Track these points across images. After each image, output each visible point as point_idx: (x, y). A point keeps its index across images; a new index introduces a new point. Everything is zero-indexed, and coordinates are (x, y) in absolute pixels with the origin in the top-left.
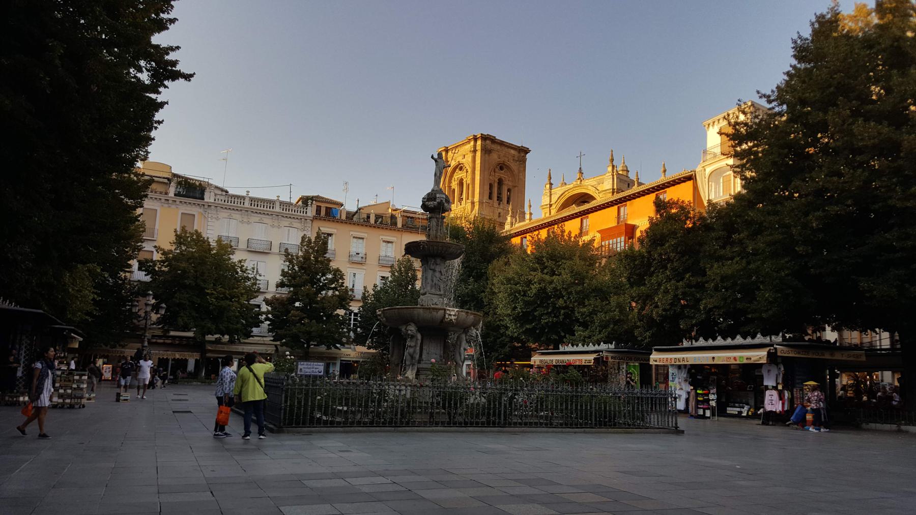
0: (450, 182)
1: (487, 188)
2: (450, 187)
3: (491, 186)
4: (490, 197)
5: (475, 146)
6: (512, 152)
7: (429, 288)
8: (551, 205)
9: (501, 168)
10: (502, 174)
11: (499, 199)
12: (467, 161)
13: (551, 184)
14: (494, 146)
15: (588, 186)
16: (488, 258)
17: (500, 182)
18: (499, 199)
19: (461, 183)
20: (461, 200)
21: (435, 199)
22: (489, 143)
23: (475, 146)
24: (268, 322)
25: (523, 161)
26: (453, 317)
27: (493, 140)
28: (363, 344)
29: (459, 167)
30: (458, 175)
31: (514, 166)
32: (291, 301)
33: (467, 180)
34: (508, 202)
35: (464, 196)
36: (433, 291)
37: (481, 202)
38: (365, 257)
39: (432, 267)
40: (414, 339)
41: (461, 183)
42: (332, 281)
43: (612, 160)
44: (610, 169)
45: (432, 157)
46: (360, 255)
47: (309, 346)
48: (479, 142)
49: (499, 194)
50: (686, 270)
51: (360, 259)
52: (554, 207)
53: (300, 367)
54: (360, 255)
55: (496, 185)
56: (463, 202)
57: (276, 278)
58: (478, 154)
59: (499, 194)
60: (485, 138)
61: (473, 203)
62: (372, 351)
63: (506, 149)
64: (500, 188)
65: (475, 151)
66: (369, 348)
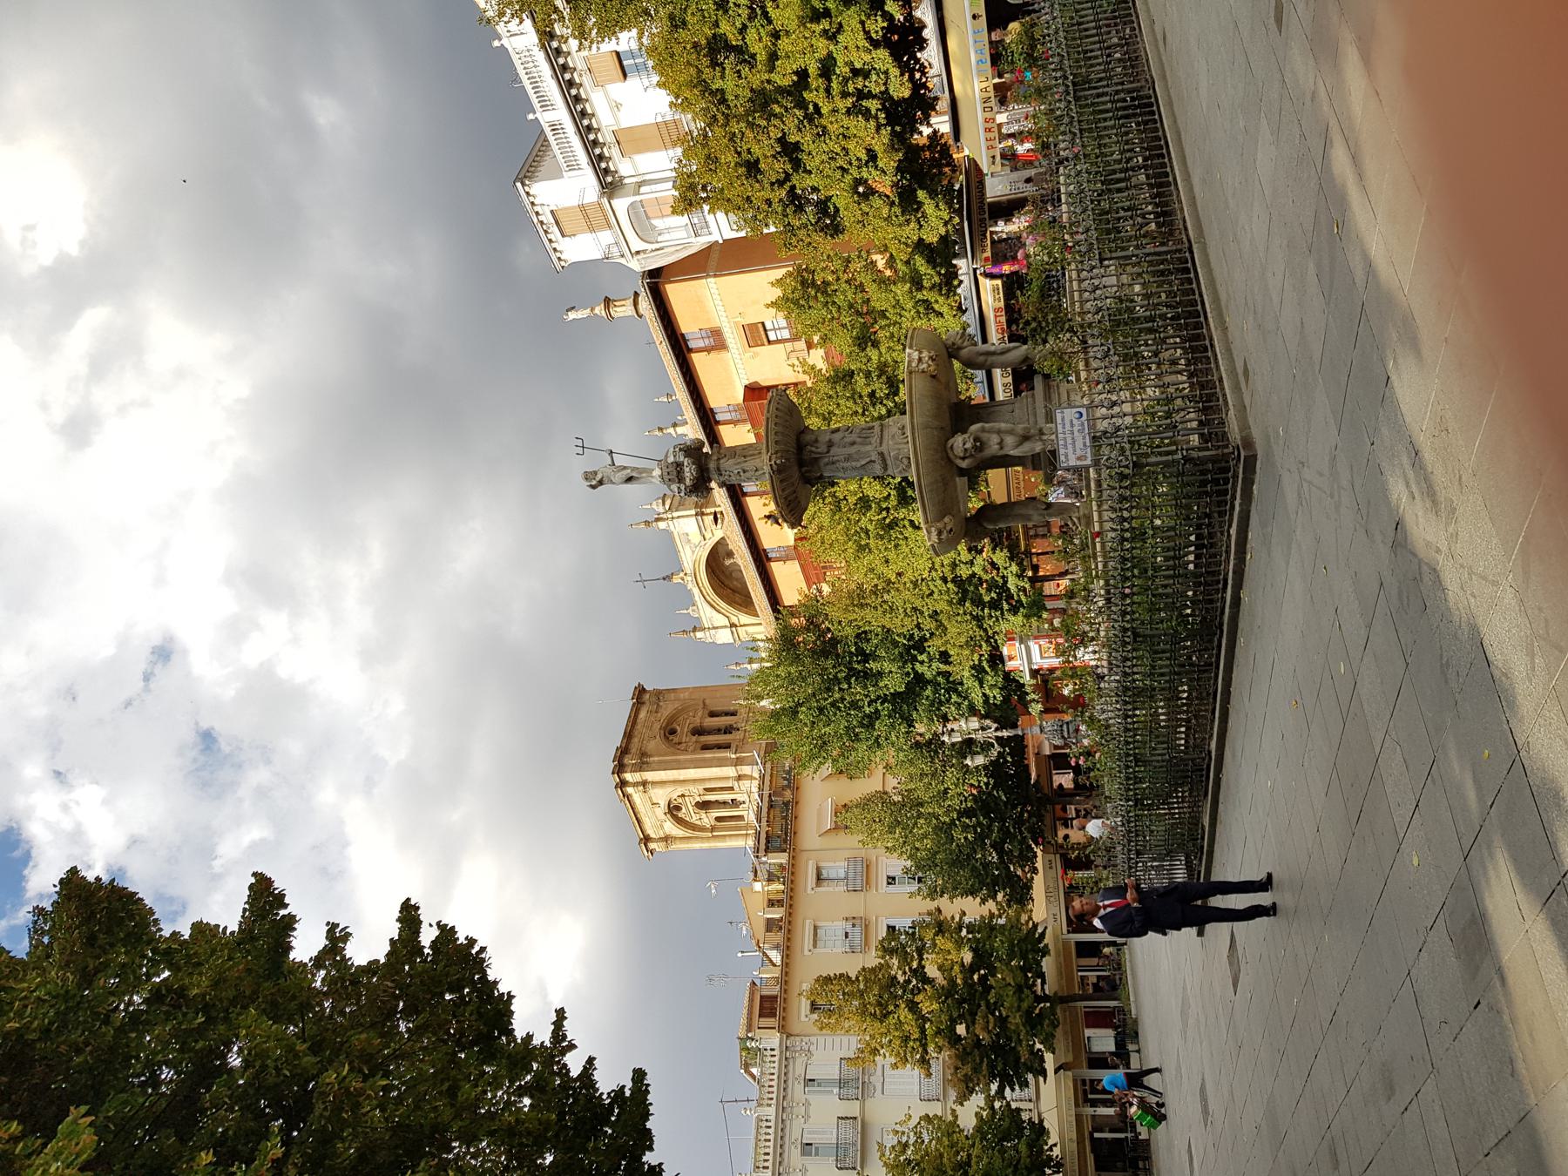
0: (702, 829)
1: (708, 755)
2: (713, 829)
3: (706, 748)
4: (727, 747)
5: (636, 785)
6: (642, 715)
7: (869, 448)
8: (733, 625)
9: (673, 732)
10: (683, 730)
11: (728, 730)
12: (662, 796)
13: (695, 630)
14: (634, 747)
15: (693, 556)
16: (828, 647)
17: (699, 732)
18: (728, 730)
19: (704, 806)
20: (735, 803)
21: (679, 465)
22: (628, 756)
23: (636, 785)
24: (1008, 1091)
25: (659, 694)
26: (925, 354)
27: (623, 751)
28: (1028, 887)
29: (673, 810)
30: (689, 812)
31: (667, 710)
32: (955, 1040)
33: (696, 793)
34: (733, 714)
35: (727, 797)
36: (875, 440)
37: (738, 762)
38: (853, 920)
39: (823, 448)
40: (985, 436)
41: (704, 806)
42: (905, 959)
43: (647, 523)
44: (662, 525)
45: (593, 487)
46: (849, 928)
47: (1045, 998)
48: (628, 776)
49: (718, 731)
50: (802, 104)
51: (857, 929)
52: (734, 620)
53: (1073, 462)
54: (849, 928)
55: (703, 739)
56: (739, 798)
57: (911, 1075)
58: (650, 776)
59: (718, 731)
60: (620, 768)
61: (739, 778)
62: (1039, 865)
63: (639, 727)
64: (709, 732)
65: (644, 783)
66: (1035, 870)
